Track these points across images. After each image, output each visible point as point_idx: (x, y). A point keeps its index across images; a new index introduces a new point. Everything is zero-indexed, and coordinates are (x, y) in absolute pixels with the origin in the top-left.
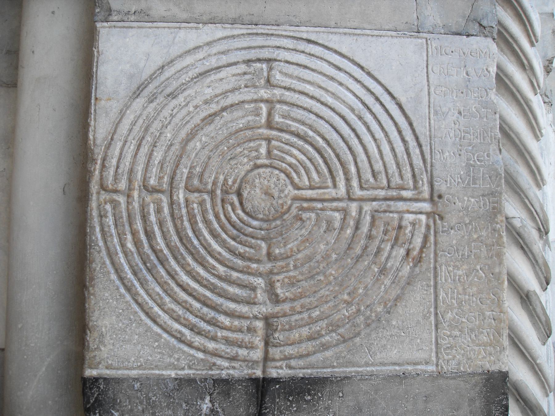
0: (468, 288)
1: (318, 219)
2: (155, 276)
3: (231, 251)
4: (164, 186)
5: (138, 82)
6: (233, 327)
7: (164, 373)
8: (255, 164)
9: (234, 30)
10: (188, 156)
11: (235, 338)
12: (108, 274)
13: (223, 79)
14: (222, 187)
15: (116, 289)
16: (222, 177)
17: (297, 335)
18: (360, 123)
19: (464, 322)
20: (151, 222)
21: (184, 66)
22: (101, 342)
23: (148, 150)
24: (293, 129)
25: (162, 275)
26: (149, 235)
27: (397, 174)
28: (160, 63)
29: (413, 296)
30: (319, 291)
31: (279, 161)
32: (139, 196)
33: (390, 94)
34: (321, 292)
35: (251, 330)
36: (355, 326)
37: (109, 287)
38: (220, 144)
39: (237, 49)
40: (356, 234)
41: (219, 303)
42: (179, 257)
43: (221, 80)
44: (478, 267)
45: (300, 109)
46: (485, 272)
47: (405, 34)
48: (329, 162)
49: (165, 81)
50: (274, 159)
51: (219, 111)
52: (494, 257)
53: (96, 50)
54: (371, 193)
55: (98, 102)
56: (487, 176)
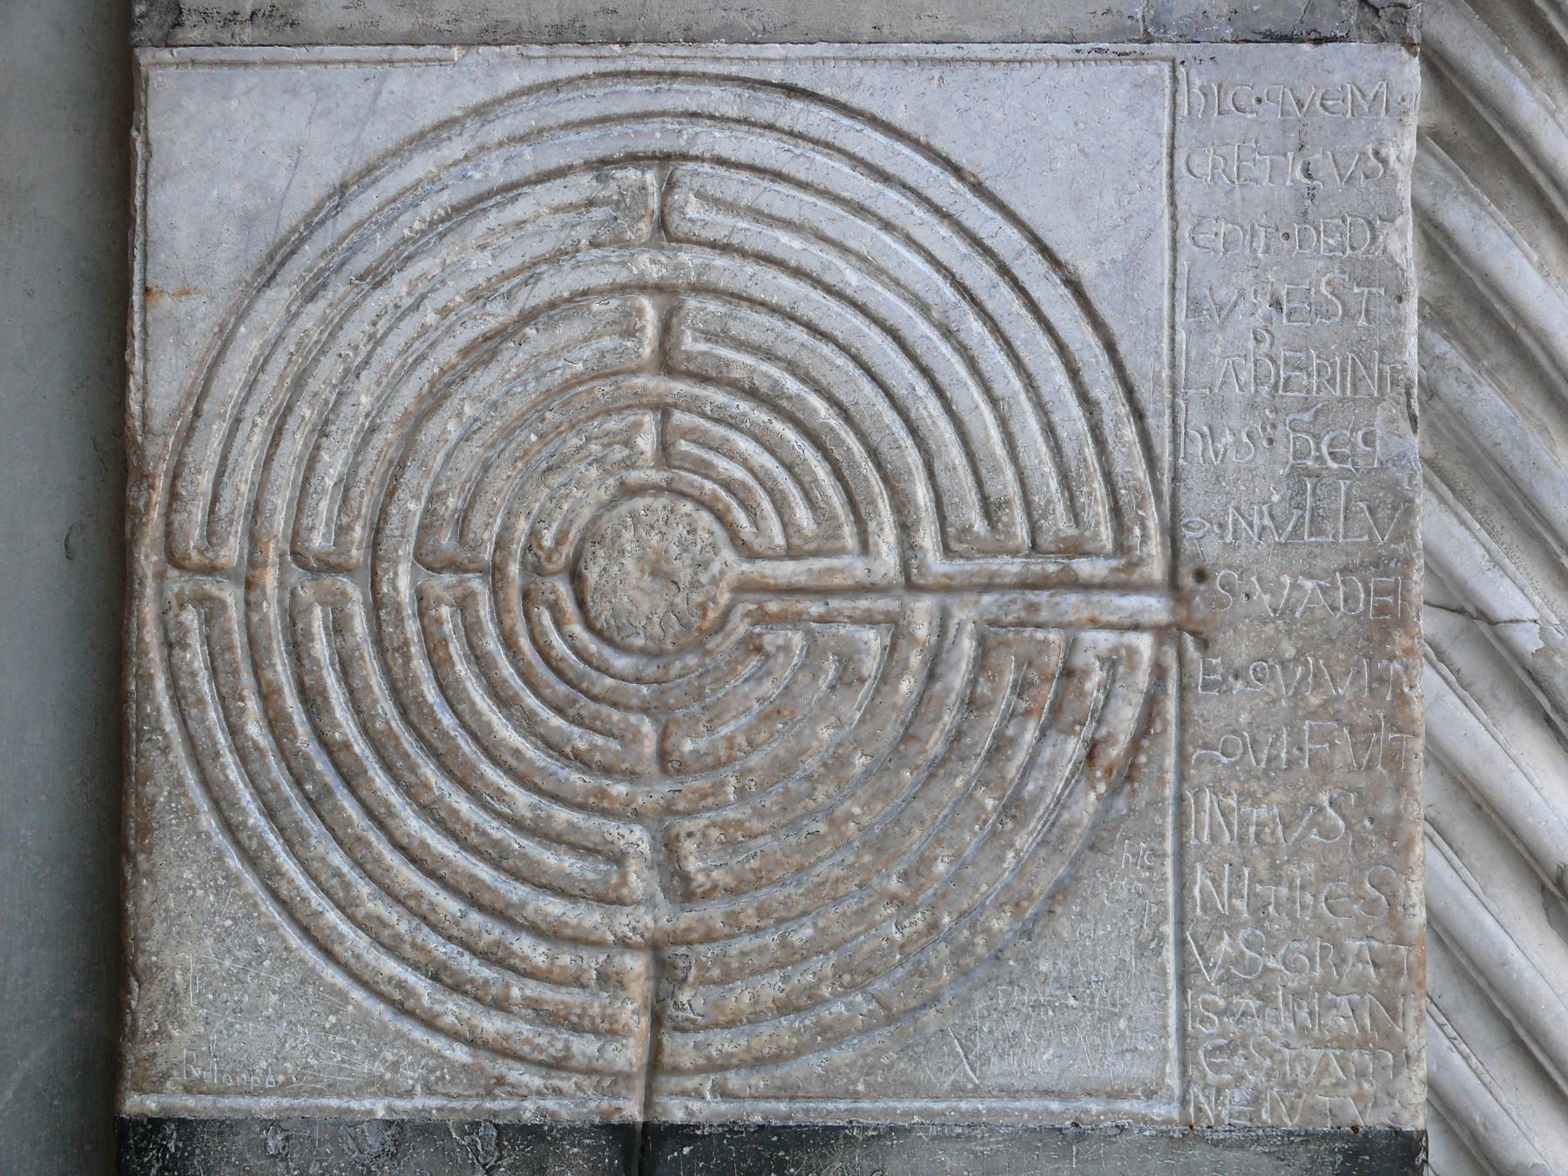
0: (1288, 862)
1: (813, 650)
2: (328, 820)
4: (354, 552)
5: (270, 239)
6: (556, 970)
7: (354, 1105)
8: (622, 483)
10: (424, 464)
12: (192, 815)
14: (524, 556)
16: (523, 526)
17: (746, 998)
18: (945, 349)
19: (1272, 970)
20: (316, 661)
21: (407, 183)
22: (172, 1015)
23: (305, 445)
24: (736, 374)
26: (312, 699)
27: (1060, 507)
28: (333, 175)
29: (1107, 885)
30: (813, 866)
31: (695, 473)
32: (282, 585)
34: (818, 870)
35: (609, 980)
36: (922, 975)
37: (194, 852)
40: (927, 695)
41: (515, 898)
43: (520, 224)
44: (1324, 798)
45: (761, 308)
46: (1347, 813)
47: (1100, 50)
48: (847, 473)
49: (351, 231)
52: (1379, 767)
54: (976, 568)
55: (151, 302)
56: (1363, 505)
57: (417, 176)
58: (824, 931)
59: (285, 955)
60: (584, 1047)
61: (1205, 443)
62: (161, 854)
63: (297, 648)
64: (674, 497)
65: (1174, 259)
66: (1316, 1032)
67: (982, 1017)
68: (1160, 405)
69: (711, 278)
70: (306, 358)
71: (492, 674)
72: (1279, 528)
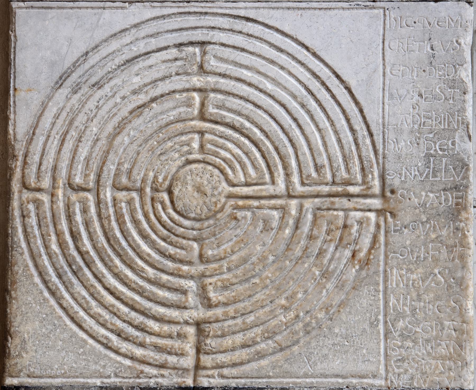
0: (424, 293)
2: (81, 279)
3: (162, 253)
4: (91, 184)
5: (60, 71)
6: (162, 332)
7: (89, 381)
8: (187, 159)
9: (164, 9)
10: (116, 152)
11: (165, 344)
13: (152, 66)
14: (152, 184)
15: (40, 293)
16: (151, 174)
17: (230, 342)
18: (302, 112)
19: (418, 332)
20: (77, 222)
21: (110, 52)
22: (23, 349)
23: (73, 145)
24: (228, 120)
25: (88, 278)
26: (75, 236)
27: (343, 168)
29: (359, 302)
30: (254, 295)
31: (213, 155)
32: (64, 195)
33: (338, 76)
34: (256, 296)
36: (293, 334)
37: (32, 291)
38: (150, 138)
39: (167, 31)
40: (295, 234)
41: (148, 307)
42: (107, 259)
43: (150, 67)
44: (436, 271)
45: (237, 97)
47: (358, 5)
50: (208, 154)
51: (149, 102)
52: (456, 260)
53: (13, 35)
55: (17, 93)
57: (113, 49)
58: (258, 318)
59: (65, 327)
60: (172, 360)
61: (395, 145)
62: (20, 291)
63: (70, 218)
64: (205, 164)
65: (384, 79)
66: (434, 354)
67: (314, 349)
68: (378, 132)
69: (218, 86)
70: (73, 114)
71: (140, 227)
72: (421, 175)
